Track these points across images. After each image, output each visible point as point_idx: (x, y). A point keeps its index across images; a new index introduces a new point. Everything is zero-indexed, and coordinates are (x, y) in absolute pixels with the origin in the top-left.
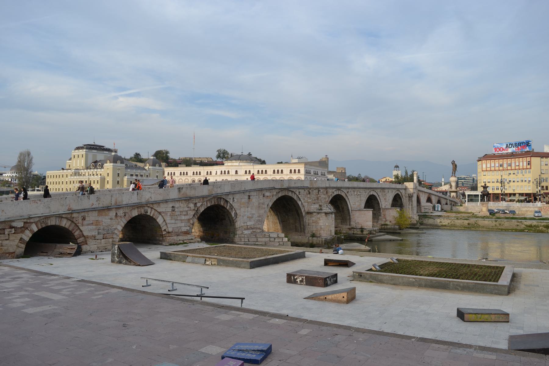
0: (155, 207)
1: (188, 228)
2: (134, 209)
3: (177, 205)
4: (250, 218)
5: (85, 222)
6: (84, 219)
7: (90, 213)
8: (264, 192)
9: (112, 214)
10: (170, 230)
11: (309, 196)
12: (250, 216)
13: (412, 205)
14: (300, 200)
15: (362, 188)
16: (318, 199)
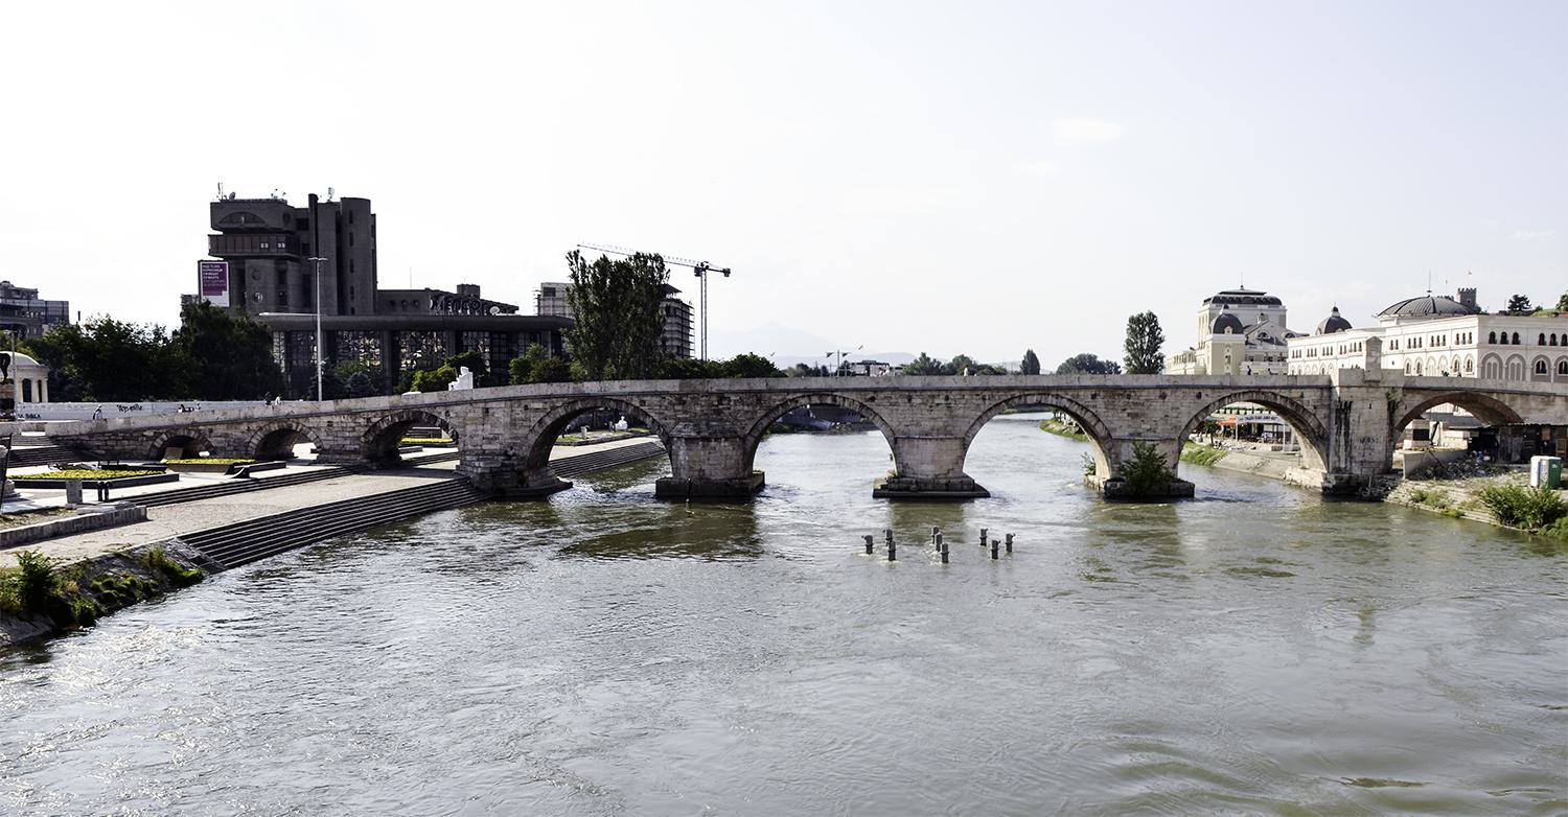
0: (301, 421)
1: (357, 447)
2: (273, 423)
3: (336, 419)
4: (490, 441)
5: (213, 434)
6: (211, 431)
7: (218, 426)
8: (524, 403)
9: (244, 427)
10: (327, 447)
11: (678, 408)
12: (491, 436)
13: (1347, 434)
14: (647, 415)
15: (961, 390)
16: (719, 412)
